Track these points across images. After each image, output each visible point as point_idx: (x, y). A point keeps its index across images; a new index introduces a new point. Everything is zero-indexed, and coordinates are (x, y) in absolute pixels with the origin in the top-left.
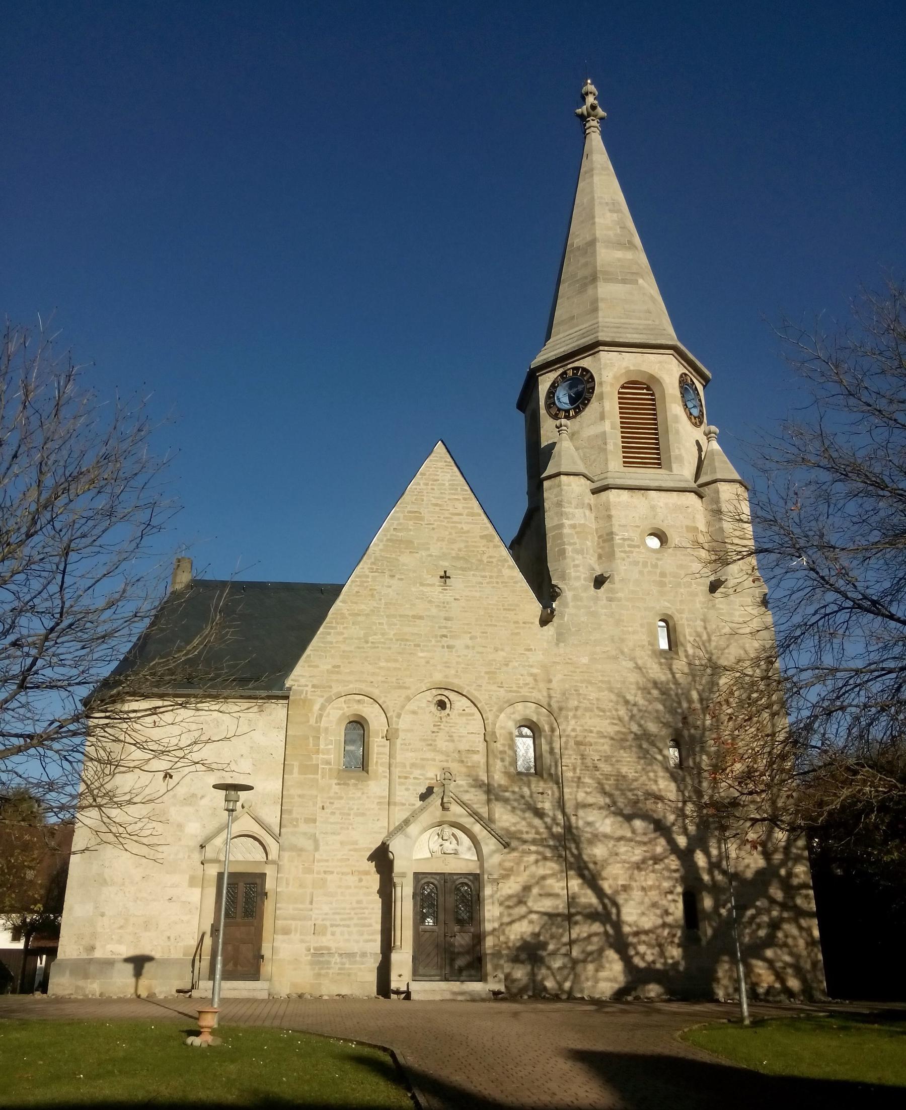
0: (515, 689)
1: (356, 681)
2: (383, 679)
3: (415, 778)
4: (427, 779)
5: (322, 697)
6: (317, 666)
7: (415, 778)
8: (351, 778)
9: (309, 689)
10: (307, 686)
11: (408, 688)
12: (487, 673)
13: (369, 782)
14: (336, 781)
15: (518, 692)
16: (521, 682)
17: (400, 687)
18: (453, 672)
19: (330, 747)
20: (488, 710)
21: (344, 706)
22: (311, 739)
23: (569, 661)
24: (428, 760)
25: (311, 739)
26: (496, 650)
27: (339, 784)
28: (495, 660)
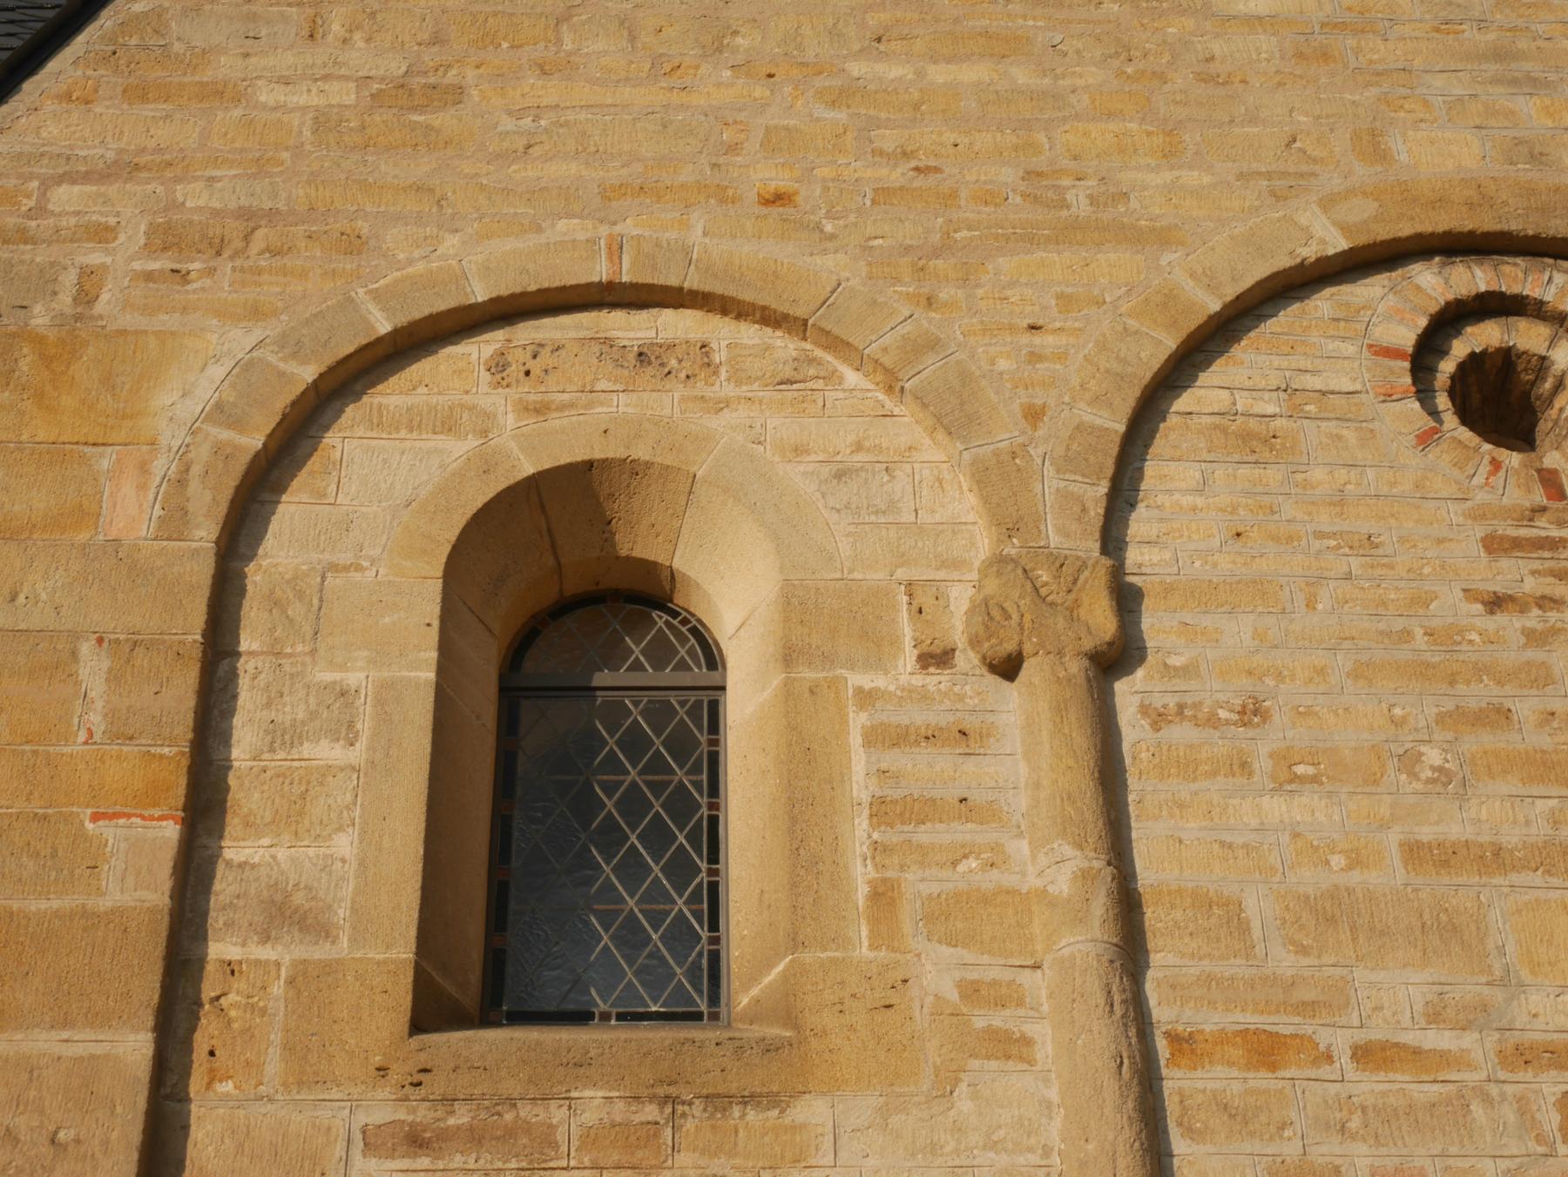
1: (609, 194)
2: (897, 175)
3: (1367, 1055)
4: (1523, 1056)
5: (256, 313)
6: (218, 93)
7: (1367, 1055)
8: (580, 1067)
9: (124, 257)
10: (102, 234)
11: (1163, 237)
13: (812, 1111)
14: (382, 1109)
17: (1069, 233)
19: (327, 752)
21: (501, 404)
22: (93, 668)
24: (1495, 859)
25: (93, 668)
27: (416, 1141)
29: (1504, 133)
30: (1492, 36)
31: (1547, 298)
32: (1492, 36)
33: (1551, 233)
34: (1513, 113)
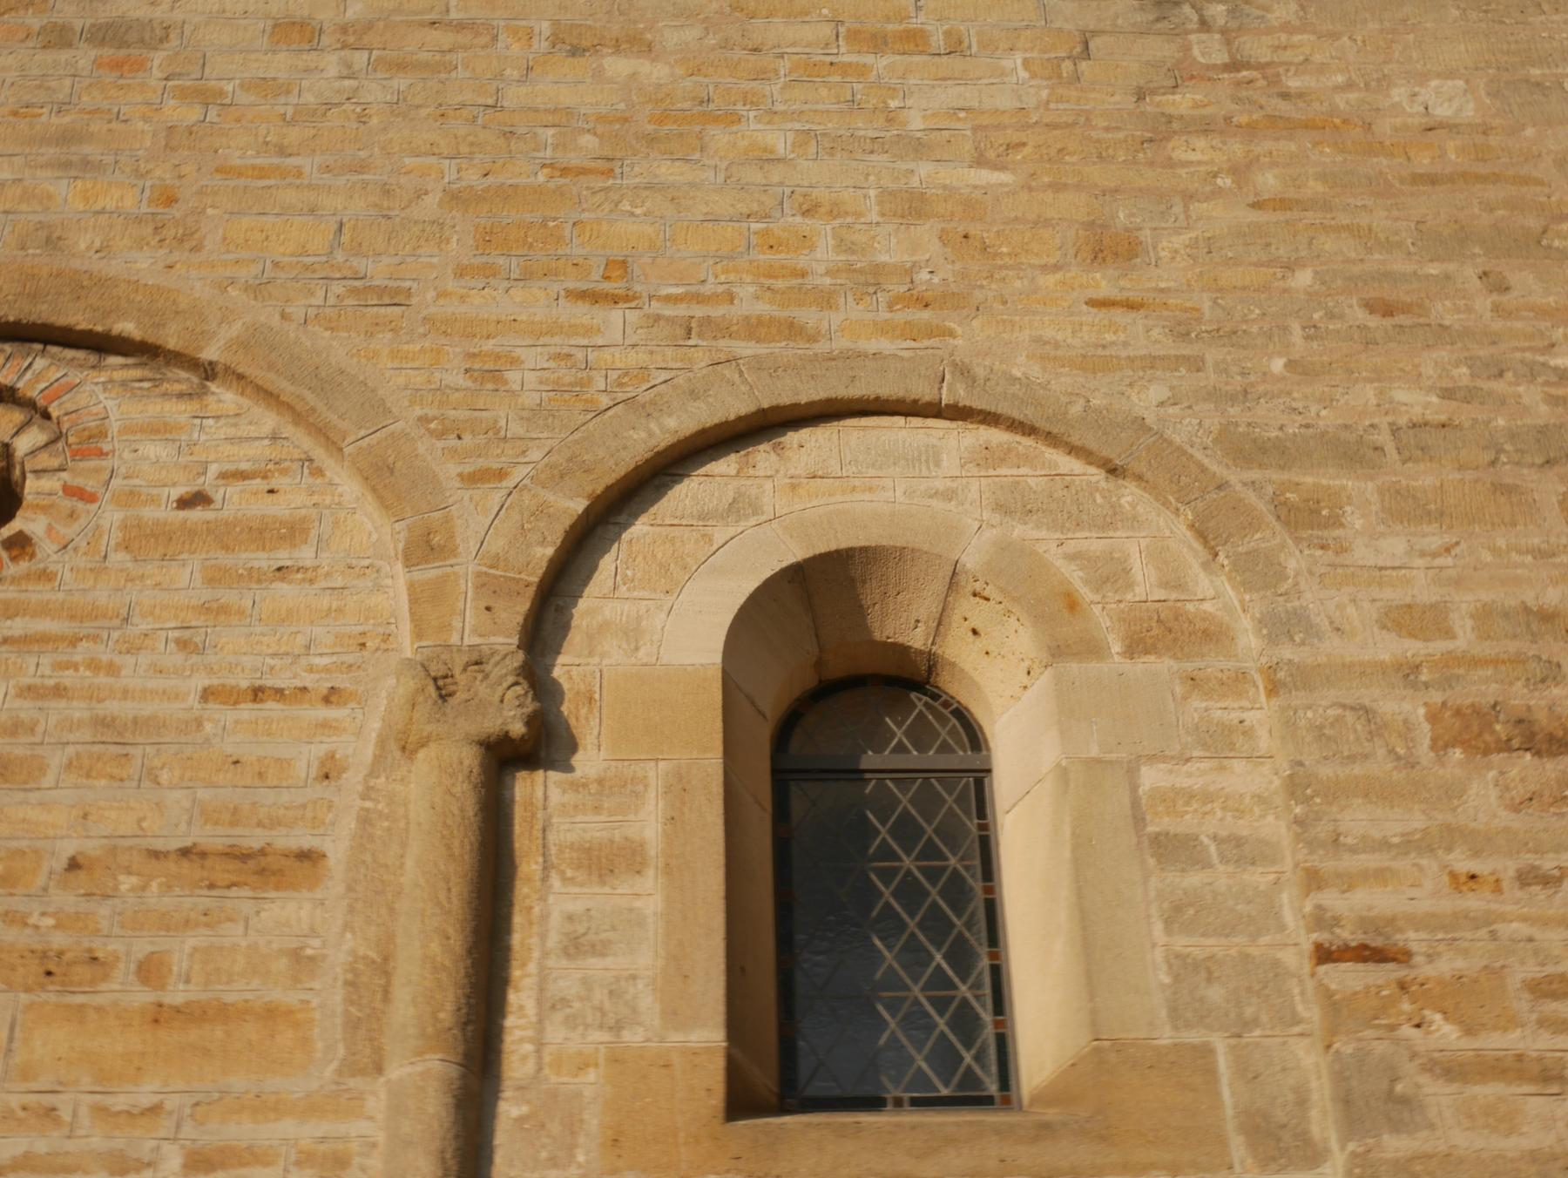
0: (750, 303)
12: (455, 198)
15: (793, 330)
16: (823, 256)
18: (123, 197)
20: (450, 471)
23: (1284, 107)
26: (574, 44)
28: (562, 117)
29: (31, 217)
30: (67, 119)
31: (20, 385)
32: (67, 119)
33: (33, 318)
34: (50, 197)
